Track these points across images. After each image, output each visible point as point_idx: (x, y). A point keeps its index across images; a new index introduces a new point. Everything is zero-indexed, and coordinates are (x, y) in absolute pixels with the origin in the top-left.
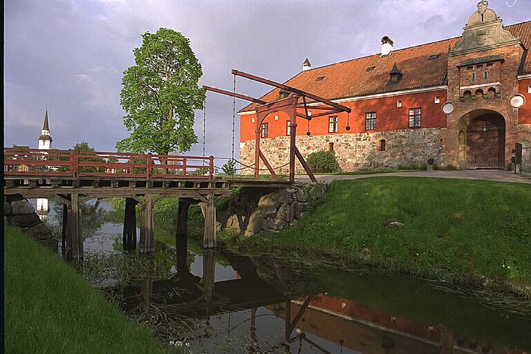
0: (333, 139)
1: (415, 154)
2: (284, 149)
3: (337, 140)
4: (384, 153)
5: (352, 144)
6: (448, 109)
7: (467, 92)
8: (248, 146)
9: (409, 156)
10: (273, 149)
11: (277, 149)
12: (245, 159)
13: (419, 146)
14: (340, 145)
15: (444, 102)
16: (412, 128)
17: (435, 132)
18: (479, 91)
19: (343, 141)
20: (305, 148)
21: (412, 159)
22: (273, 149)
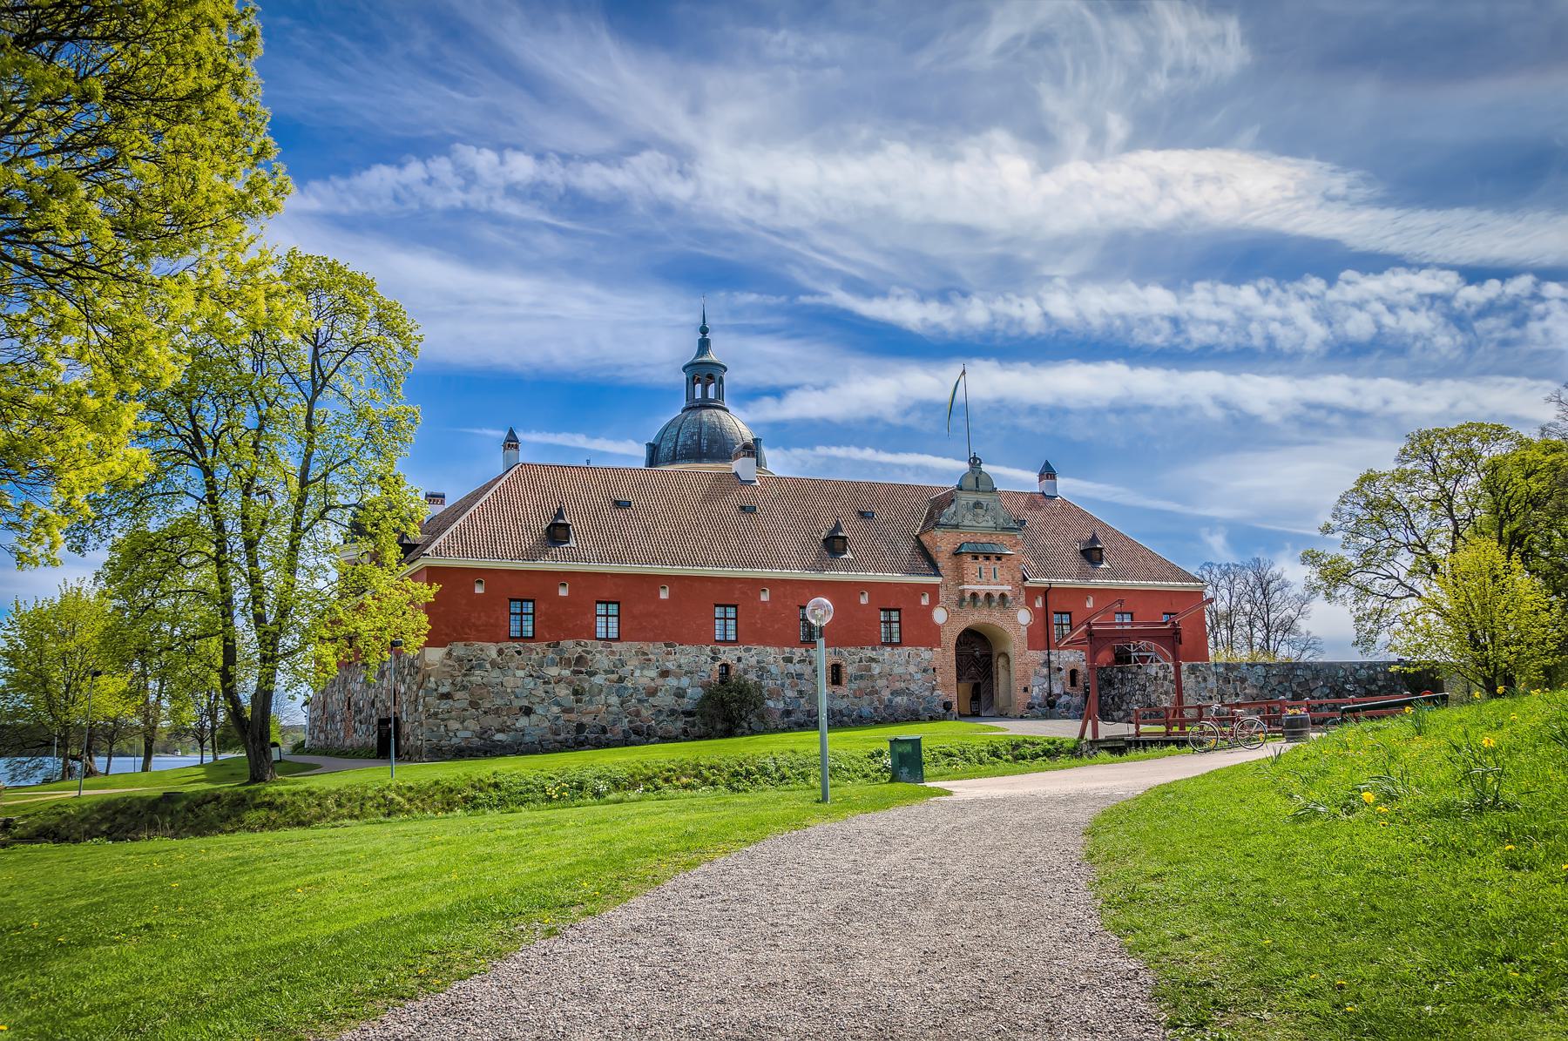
0: (728, 655)
1: (895, 693)
2: (592, 674)
3: (739, 659)
4: (840, 690)
5: (773, 669)
6: (939, 616)
7: (974, 595)
8: (460, 660)
9: (886, 694)
10: (553, 671)
11: (566, 673)
12: (447, 696)
13: (901, 678)
14: (746, 671)
15: (935, 601)
16: (884, 644)
17: (925, 654)
18: (989, 596)
19: (753, 661)
20: (653, 673)
21: (890, 701)
22: (553, 671)
